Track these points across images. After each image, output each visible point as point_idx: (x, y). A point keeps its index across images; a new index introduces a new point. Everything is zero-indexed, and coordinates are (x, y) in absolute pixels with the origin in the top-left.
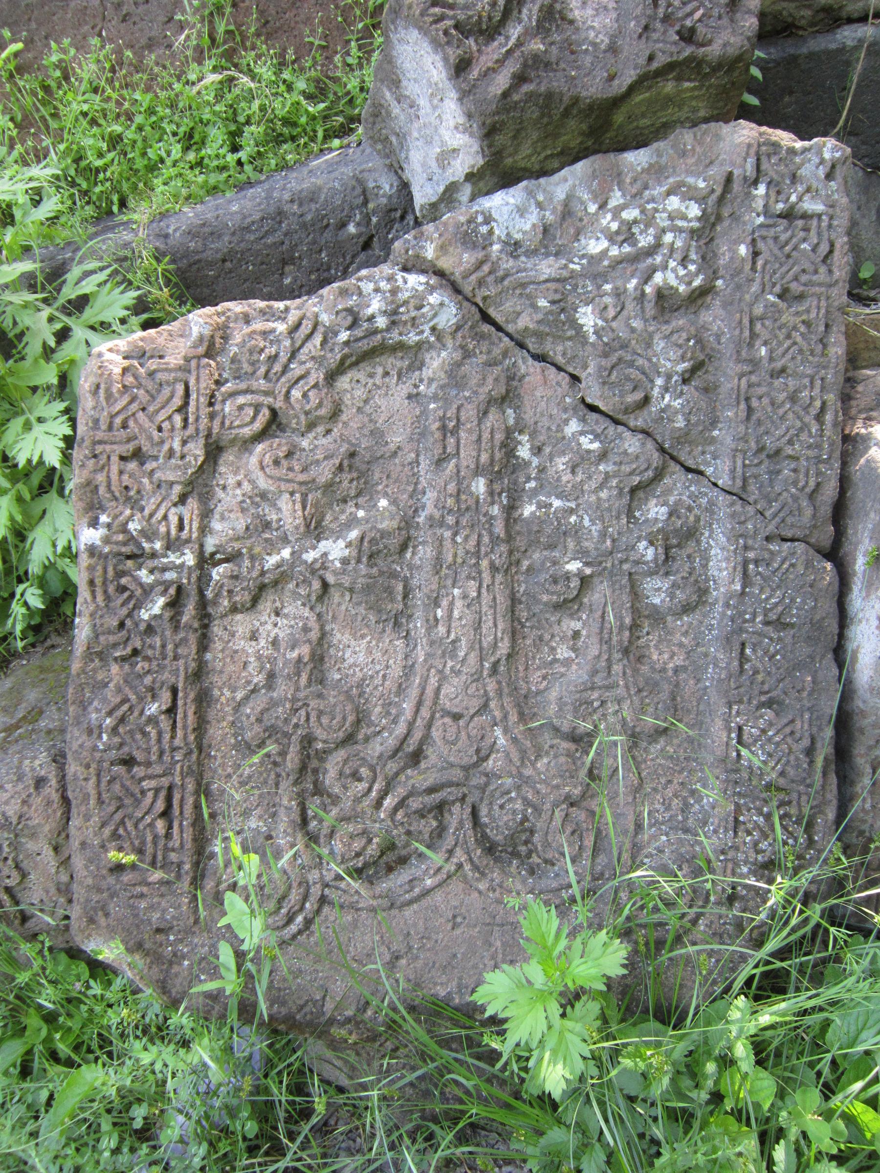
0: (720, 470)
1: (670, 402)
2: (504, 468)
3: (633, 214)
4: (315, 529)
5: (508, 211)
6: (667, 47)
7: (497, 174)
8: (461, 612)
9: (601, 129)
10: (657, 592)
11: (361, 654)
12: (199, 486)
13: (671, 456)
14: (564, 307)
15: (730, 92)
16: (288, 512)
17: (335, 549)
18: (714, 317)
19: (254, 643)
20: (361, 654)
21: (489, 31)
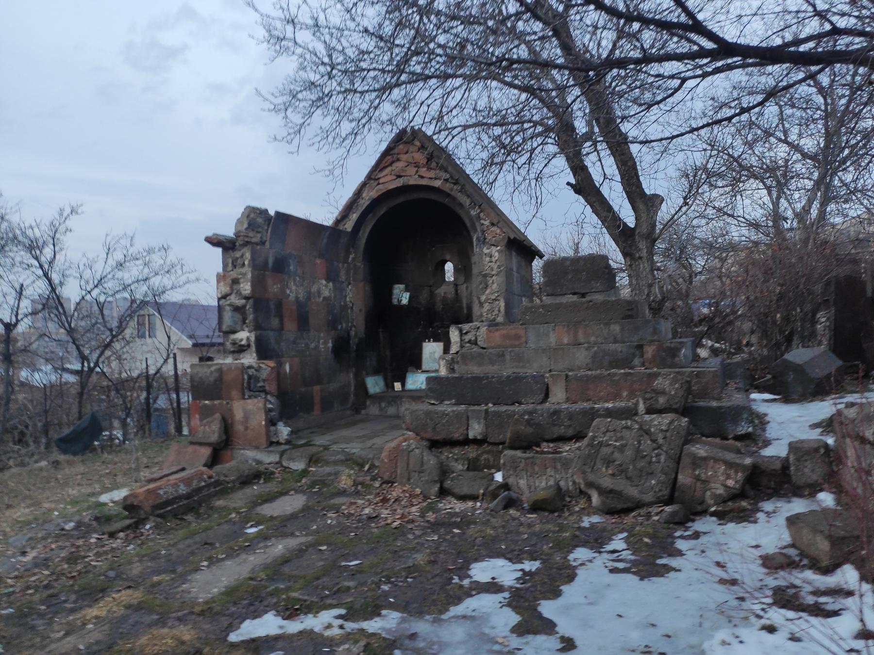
0: (664, 449)
1: (661, 441)
2: (639, 442)
3: (664, 420)
4: (616, 441)
5: (647, 417)
6: (667, 405)
7: (647, 413)
8: (629, 453)
9: (660, 412)
10: (654, 459)
11: (617, 455)
12: (604, 433)
13: (659, 447)
14: (650, 427)
15: (675, 411)
16: (614, 438)
17: (618, 444)
18: (668, 434)
19: (605, 451)
20: (617, 455)
21: (649, 399)
